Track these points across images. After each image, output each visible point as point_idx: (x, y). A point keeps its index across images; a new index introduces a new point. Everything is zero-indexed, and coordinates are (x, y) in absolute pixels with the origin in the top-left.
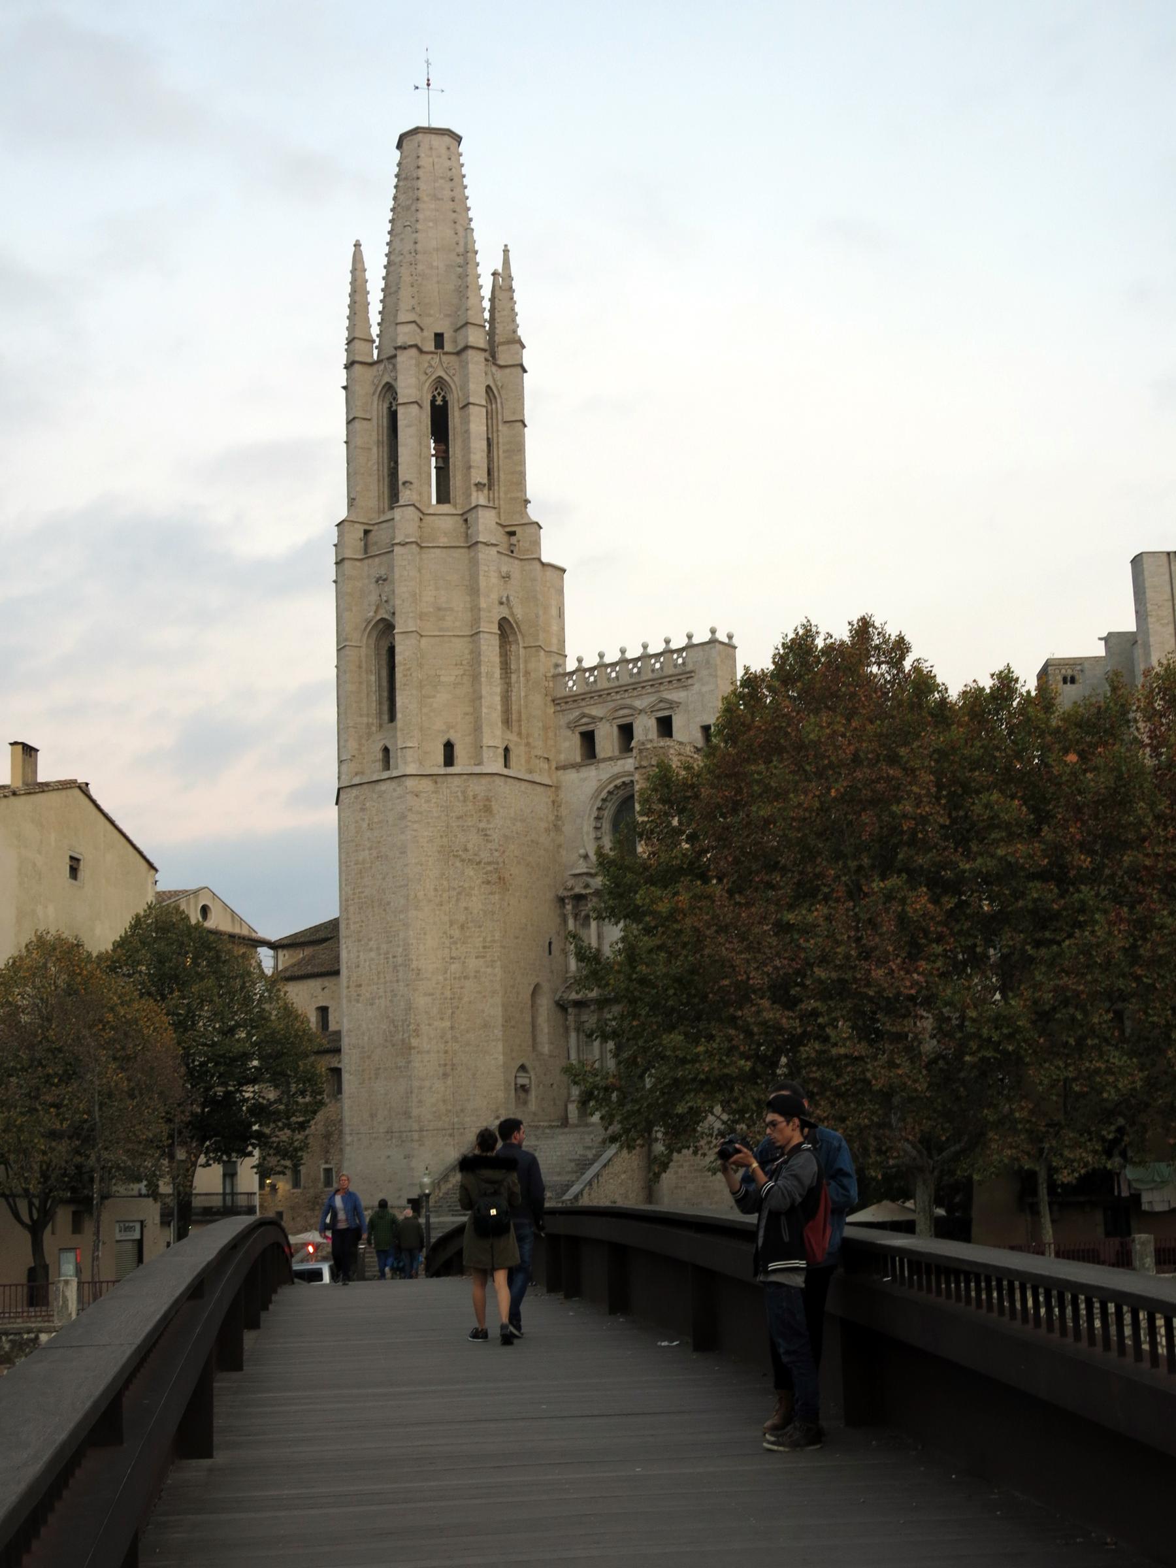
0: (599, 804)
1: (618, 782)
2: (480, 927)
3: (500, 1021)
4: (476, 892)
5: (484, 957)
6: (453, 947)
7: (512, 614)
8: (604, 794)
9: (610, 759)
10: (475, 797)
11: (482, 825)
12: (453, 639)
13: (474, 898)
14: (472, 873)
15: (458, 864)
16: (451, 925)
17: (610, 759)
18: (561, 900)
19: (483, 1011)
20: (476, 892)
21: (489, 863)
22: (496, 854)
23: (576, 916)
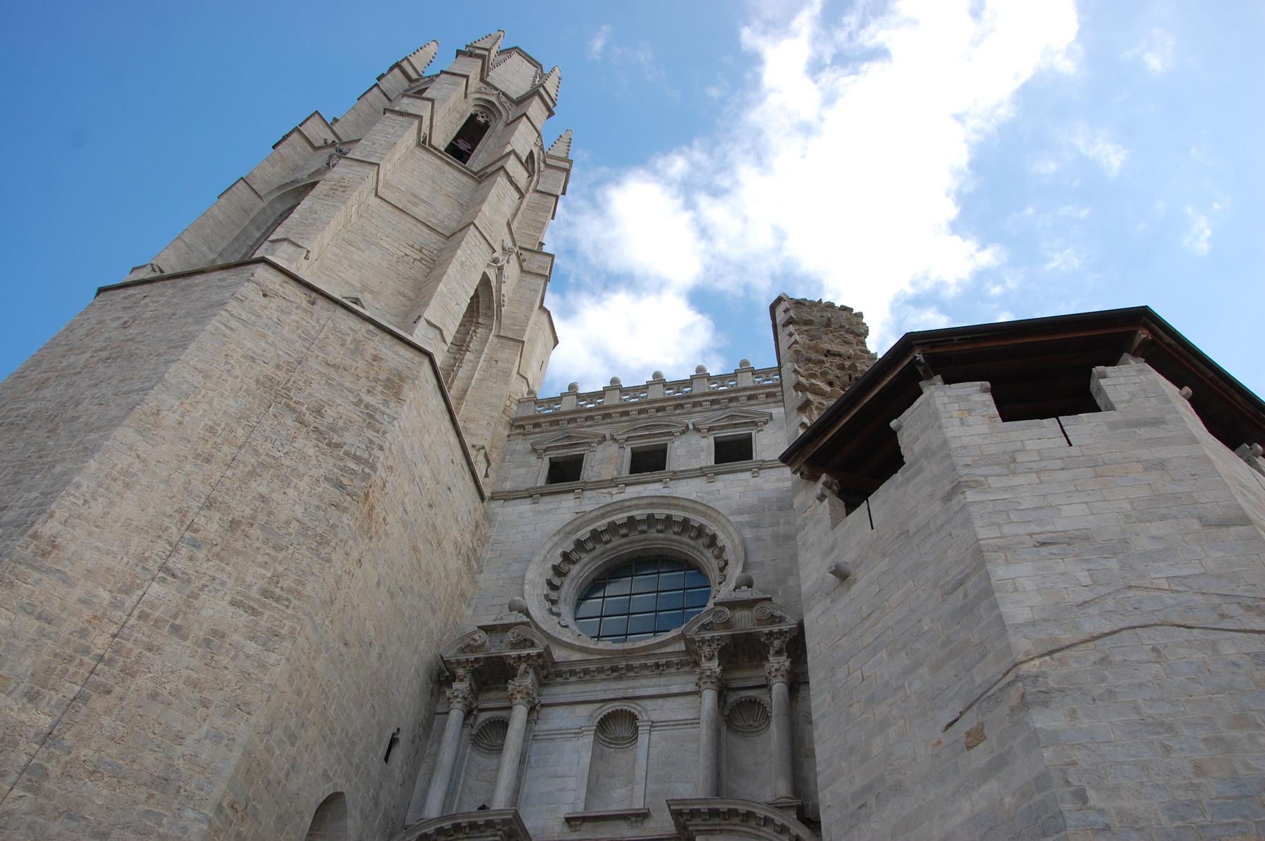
0: (569, 546)
1: (620, 517)
2: (277, 548)
3: (219, 790)
4: (303, 485)
5: (254, 612)
6: (184, 551)
7: (499, 290)
8: (584, 534)
9: (614, 483)
10: (376, 358)
11: (367, 399)
12: (420, 226)
13: (291, 492)
14: (311, 452)
15: (289, 421)
16: (210, 504)
17: (614, 483)
18: (441, 677)
19: (180, 738)
20: (303, 485)
21: (356, 458)
22: (376, 452)
23: (469, 713)
